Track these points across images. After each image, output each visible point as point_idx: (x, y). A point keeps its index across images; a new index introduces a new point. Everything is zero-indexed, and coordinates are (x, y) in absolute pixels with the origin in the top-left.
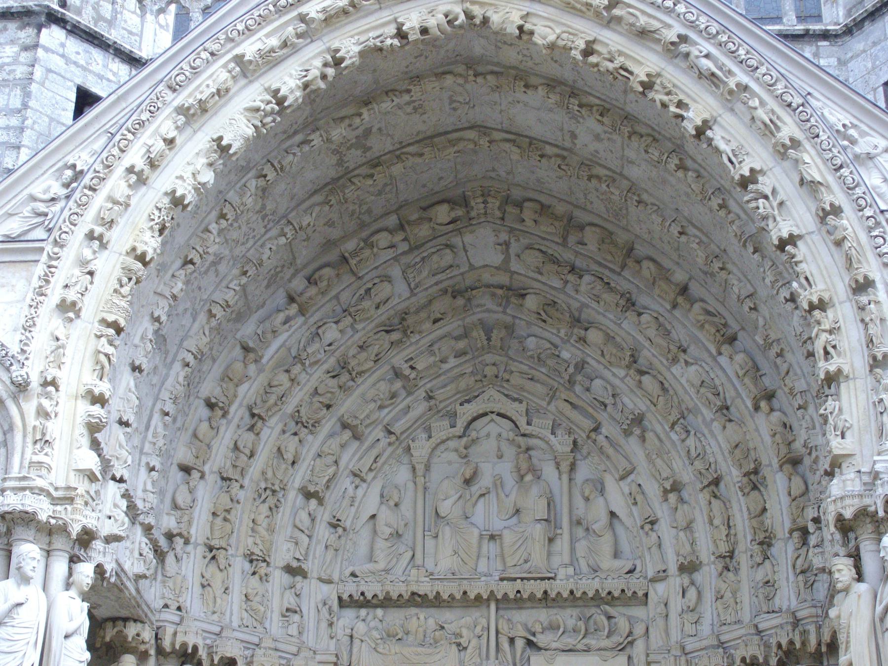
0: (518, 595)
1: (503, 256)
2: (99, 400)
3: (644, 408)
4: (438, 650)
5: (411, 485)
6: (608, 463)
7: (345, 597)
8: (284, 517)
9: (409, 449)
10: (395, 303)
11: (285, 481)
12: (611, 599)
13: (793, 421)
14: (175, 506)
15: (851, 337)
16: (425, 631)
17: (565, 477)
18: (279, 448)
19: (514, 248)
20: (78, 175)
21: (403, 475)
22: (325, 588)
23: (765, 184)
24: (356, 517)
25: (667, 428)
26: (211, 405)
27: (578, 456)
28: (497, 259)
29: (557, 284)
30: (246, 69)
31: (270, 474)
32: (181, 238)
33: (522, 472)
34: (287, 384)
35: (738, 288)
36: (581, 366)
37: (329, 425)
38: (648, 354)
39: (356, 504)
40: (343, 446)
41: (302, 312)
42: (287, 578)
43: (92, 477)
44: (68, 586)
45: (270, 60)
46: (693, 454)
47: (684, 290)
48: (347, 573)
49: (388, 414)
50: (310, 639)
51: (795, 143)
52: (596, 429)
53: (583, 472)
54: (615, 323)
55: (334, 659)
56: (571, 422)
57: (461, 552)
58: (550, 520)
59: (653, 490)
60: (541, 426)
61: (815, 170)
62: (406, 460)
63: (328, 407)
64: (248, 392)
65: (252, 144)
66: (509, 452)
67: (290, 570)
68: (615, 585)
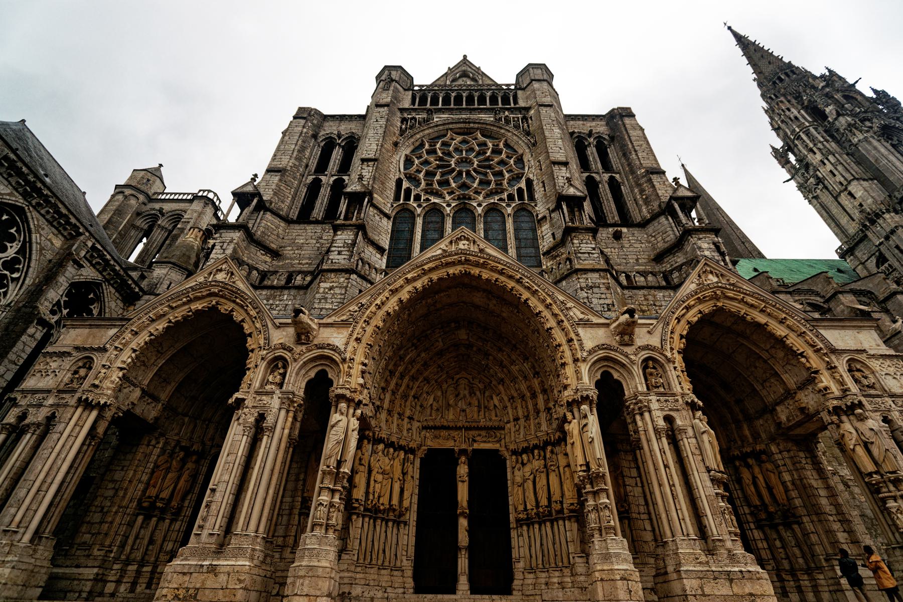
2: (365, 365)
8: (408, 403)
12: (495, 428)
13: (544, 380)
14: (380, 399)
15: (568, 354)
20: (363, 305)
21: (439, 393)
22: (418, 424)
23: (543, 314)
26: (391, 372)
30: (408, 281)
32: (387, 325)
35: (531, 344)
36: (487, 365)
38: (506, 362)
41: (416, 348)
43: (361, 385)
44: (353, 416)
45: (414, 279)
47: (515, 346)
50: (414, 437)
51: (551, 304)
52: (491, 382)
53: (487, 394)
58: (479, 407)
59: (506, 398)
60: (476, 382)
61: (557, 311)
64: (401, 369)
65: (409, 300)
66: (467, 388)
68: (496, 424)
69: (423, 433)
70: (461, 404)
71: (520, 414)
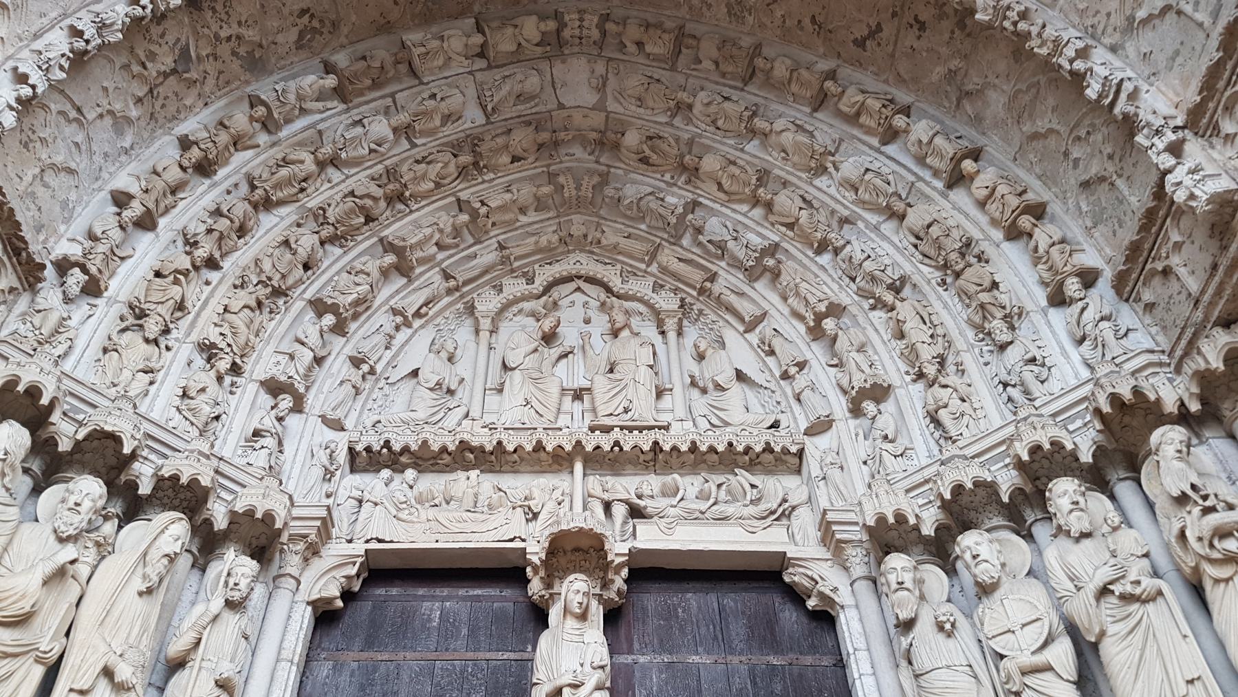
0: (616, 449)
1: (598, 96)
3: (777, 239)
4: (493, 517)
5: (472, 345)
6: (728, 317)
7: (359, 448)
9: (471, 309)
10: (466, 126)
11: (290, 281)
16: (476, 495)
17: (672, 335)
18: (286, 243)
19: (612, 82)
21: (464, 333)
22: (330, 435)
24: (392, 365)
25: (810, 253)
27: (685, 322)
28: (591, 98)
29: (663, 119)
31: (267, 265)
33: (618, 325)
34: (310, 166)
36: (694, 205)
37: (365, 242)
39: (394, 349)
40: (385, 273)
42: (266, 400)
46: (859, 256)
48: (369, 424)
49: (449, 258)
52: (713, 278)
54: (736, 149)
55: (324, 513)
56: (679, 280)
57: (535, 403)
59: (796, 331)
60: (641, 287)
62: (469, 322)
63: (369, 219)
67: (274, 388)
69: (350, 484)
70: (574, 373)
71: (892, 369)
